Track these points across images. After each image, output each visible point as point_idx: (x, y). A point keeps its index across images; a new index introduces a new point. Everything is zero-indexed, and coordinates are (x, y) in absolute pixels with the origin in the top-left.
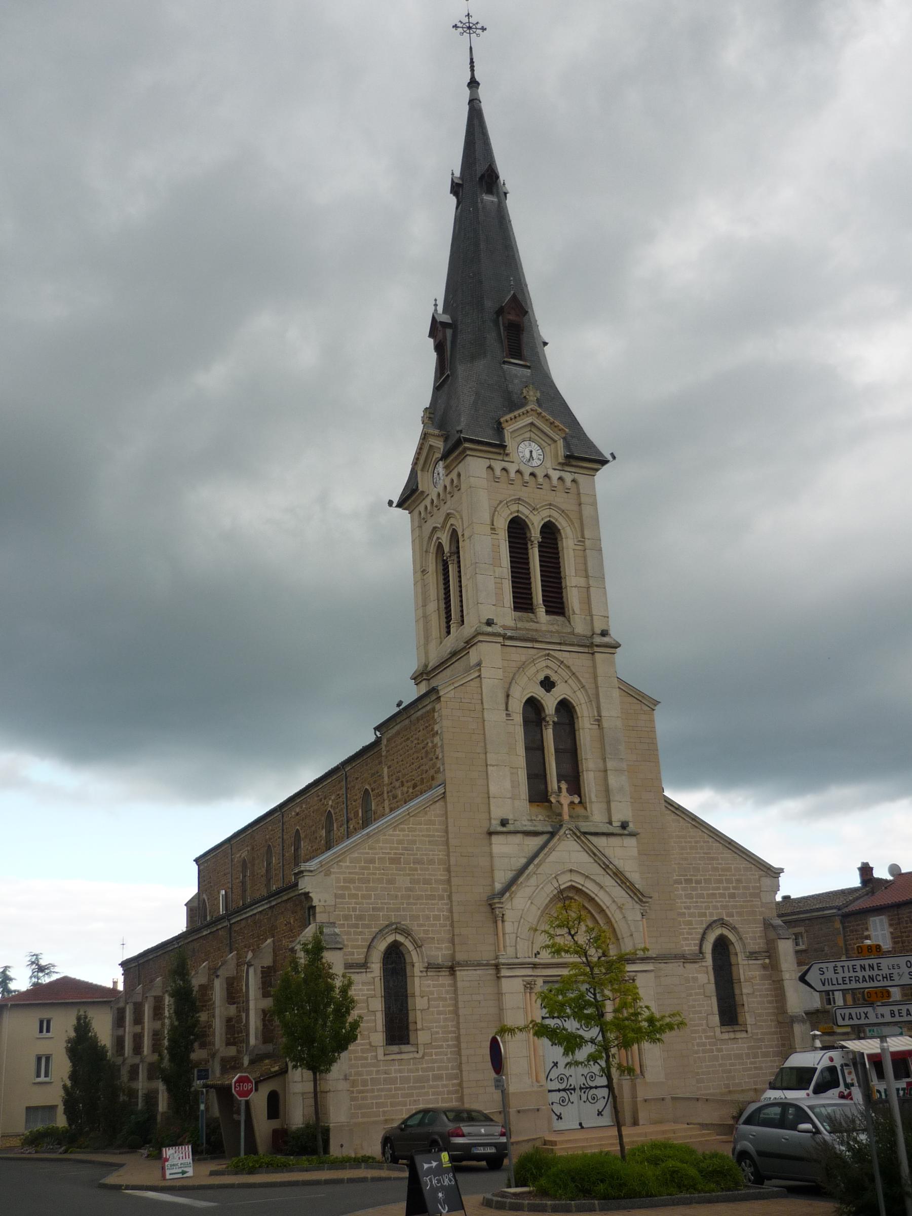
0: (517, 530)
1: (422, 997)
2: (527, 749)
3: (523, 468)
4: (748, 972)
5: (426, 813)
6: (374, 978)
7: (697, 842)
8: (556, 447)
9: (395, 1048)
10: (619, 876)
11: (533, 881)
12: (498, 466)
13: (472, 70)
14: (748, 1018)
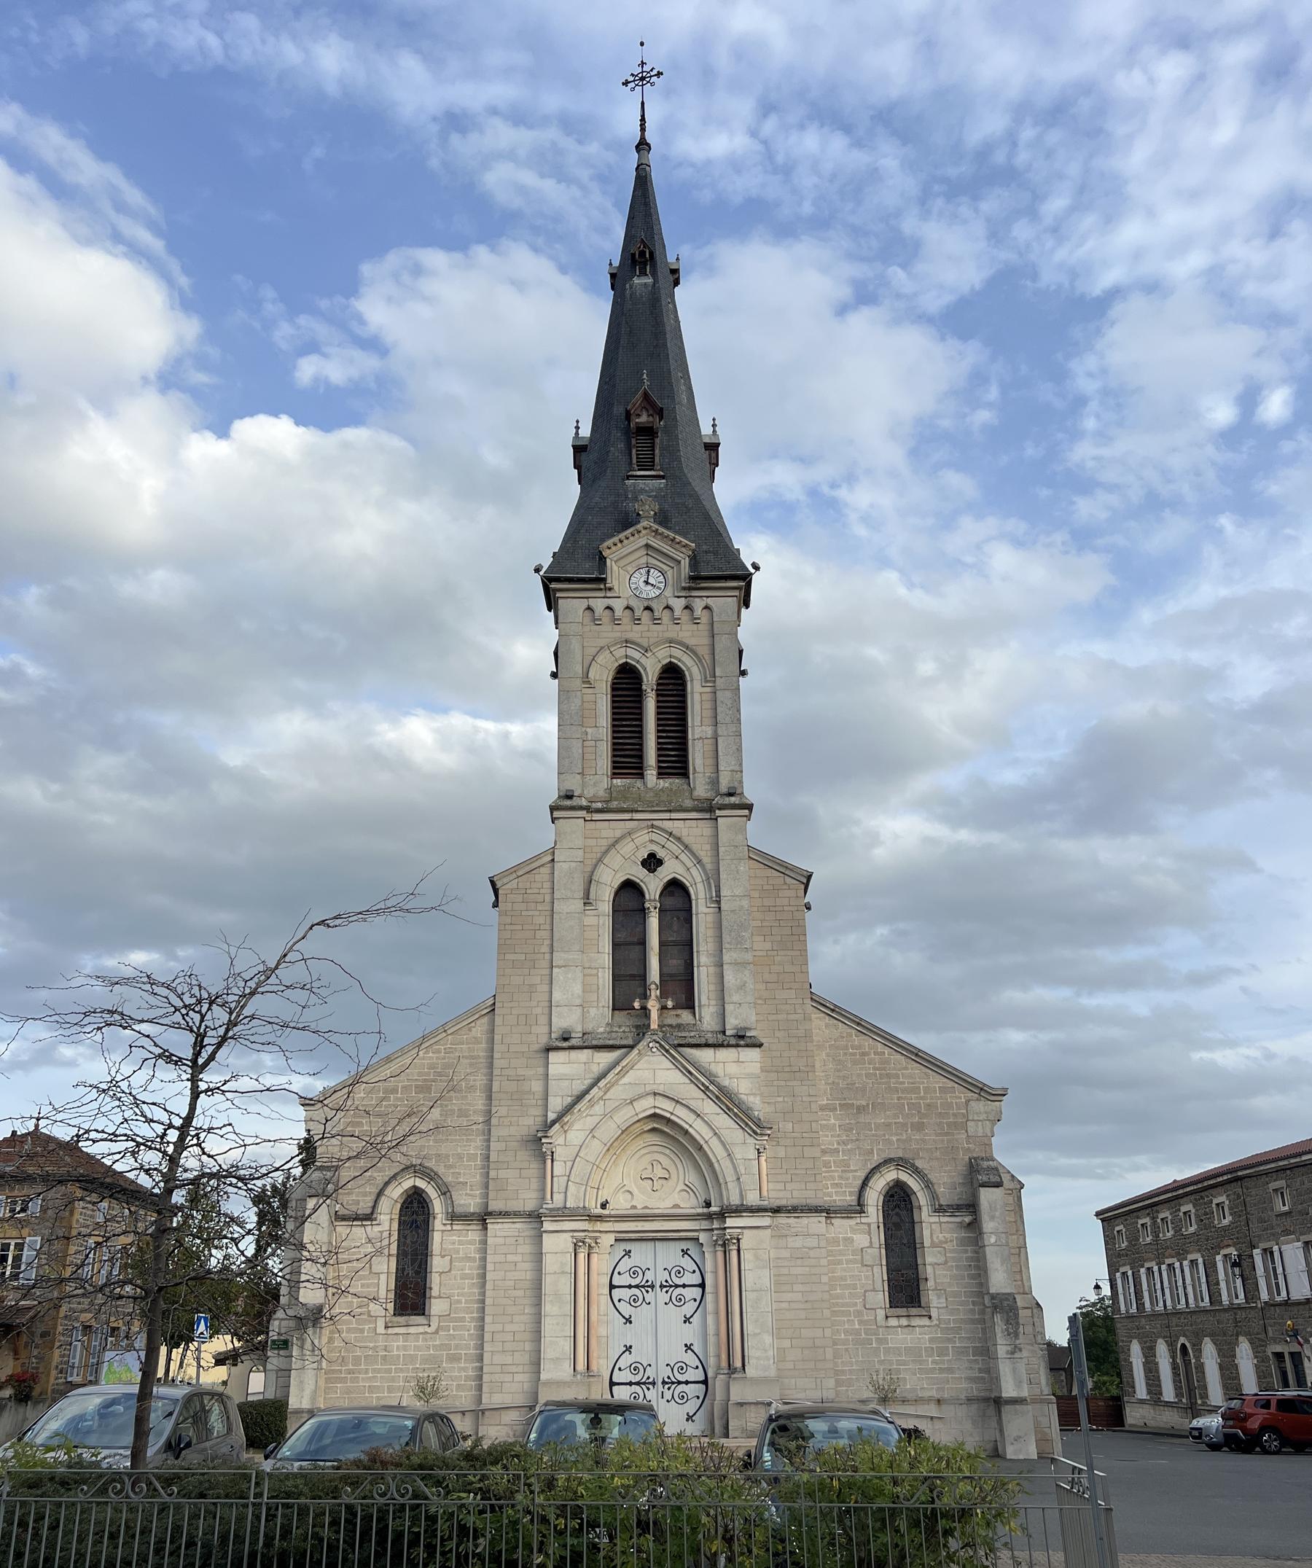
0: (627, 679)
1: (443, 1257)
2: (616, 945)
3: (633, 603)
4: (935, 1233)
5: (470, 1030)
6: (381, 1232)
7: (863, 1054)
8: (679, 570)
9: (402, 1320)
10: (726, 1099)
11: (598, 1109)
12: (598, 605)
13: (643, 129)
14: (933, 1299)
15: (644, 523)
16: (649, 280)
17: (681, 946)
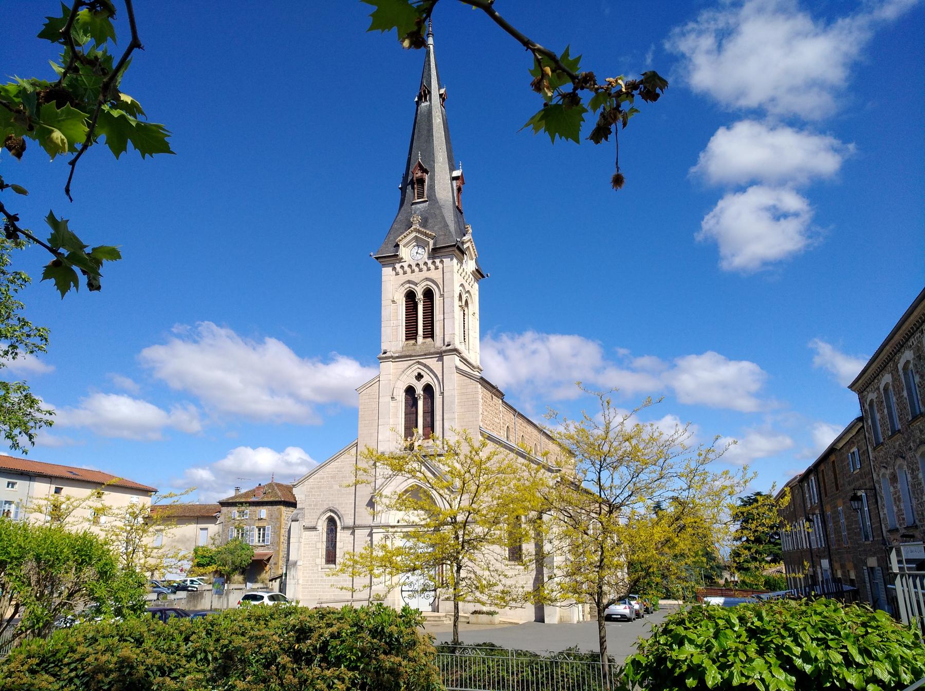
0: (410, 296)
12: (398, 266)
15: (414, 227)
16: (428, 103)
17: (430, 413)
